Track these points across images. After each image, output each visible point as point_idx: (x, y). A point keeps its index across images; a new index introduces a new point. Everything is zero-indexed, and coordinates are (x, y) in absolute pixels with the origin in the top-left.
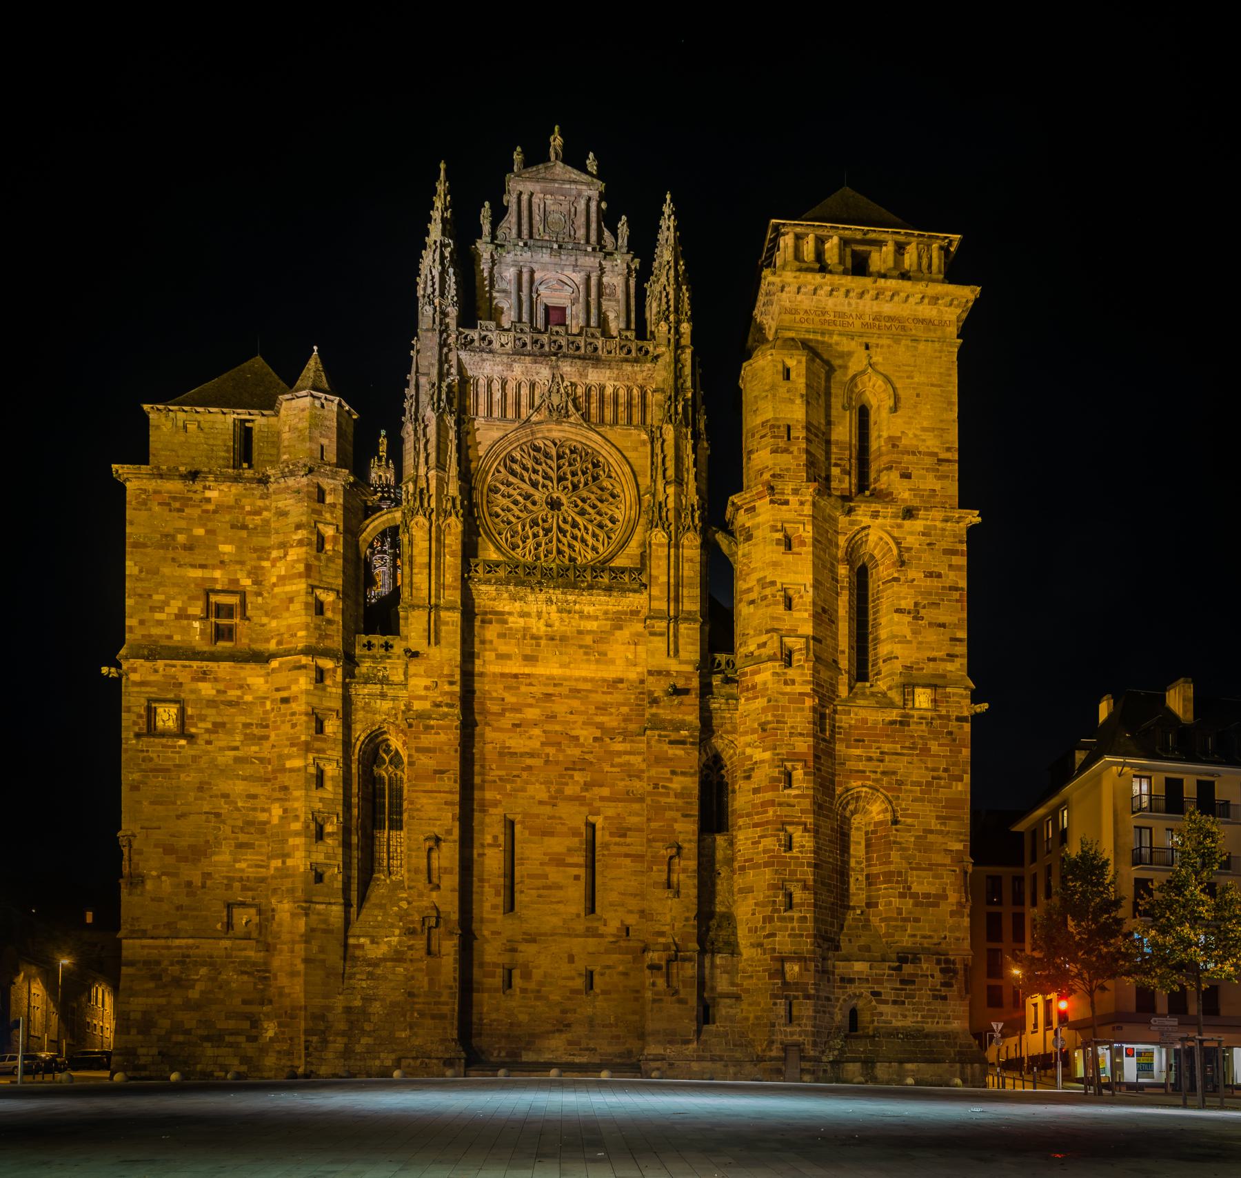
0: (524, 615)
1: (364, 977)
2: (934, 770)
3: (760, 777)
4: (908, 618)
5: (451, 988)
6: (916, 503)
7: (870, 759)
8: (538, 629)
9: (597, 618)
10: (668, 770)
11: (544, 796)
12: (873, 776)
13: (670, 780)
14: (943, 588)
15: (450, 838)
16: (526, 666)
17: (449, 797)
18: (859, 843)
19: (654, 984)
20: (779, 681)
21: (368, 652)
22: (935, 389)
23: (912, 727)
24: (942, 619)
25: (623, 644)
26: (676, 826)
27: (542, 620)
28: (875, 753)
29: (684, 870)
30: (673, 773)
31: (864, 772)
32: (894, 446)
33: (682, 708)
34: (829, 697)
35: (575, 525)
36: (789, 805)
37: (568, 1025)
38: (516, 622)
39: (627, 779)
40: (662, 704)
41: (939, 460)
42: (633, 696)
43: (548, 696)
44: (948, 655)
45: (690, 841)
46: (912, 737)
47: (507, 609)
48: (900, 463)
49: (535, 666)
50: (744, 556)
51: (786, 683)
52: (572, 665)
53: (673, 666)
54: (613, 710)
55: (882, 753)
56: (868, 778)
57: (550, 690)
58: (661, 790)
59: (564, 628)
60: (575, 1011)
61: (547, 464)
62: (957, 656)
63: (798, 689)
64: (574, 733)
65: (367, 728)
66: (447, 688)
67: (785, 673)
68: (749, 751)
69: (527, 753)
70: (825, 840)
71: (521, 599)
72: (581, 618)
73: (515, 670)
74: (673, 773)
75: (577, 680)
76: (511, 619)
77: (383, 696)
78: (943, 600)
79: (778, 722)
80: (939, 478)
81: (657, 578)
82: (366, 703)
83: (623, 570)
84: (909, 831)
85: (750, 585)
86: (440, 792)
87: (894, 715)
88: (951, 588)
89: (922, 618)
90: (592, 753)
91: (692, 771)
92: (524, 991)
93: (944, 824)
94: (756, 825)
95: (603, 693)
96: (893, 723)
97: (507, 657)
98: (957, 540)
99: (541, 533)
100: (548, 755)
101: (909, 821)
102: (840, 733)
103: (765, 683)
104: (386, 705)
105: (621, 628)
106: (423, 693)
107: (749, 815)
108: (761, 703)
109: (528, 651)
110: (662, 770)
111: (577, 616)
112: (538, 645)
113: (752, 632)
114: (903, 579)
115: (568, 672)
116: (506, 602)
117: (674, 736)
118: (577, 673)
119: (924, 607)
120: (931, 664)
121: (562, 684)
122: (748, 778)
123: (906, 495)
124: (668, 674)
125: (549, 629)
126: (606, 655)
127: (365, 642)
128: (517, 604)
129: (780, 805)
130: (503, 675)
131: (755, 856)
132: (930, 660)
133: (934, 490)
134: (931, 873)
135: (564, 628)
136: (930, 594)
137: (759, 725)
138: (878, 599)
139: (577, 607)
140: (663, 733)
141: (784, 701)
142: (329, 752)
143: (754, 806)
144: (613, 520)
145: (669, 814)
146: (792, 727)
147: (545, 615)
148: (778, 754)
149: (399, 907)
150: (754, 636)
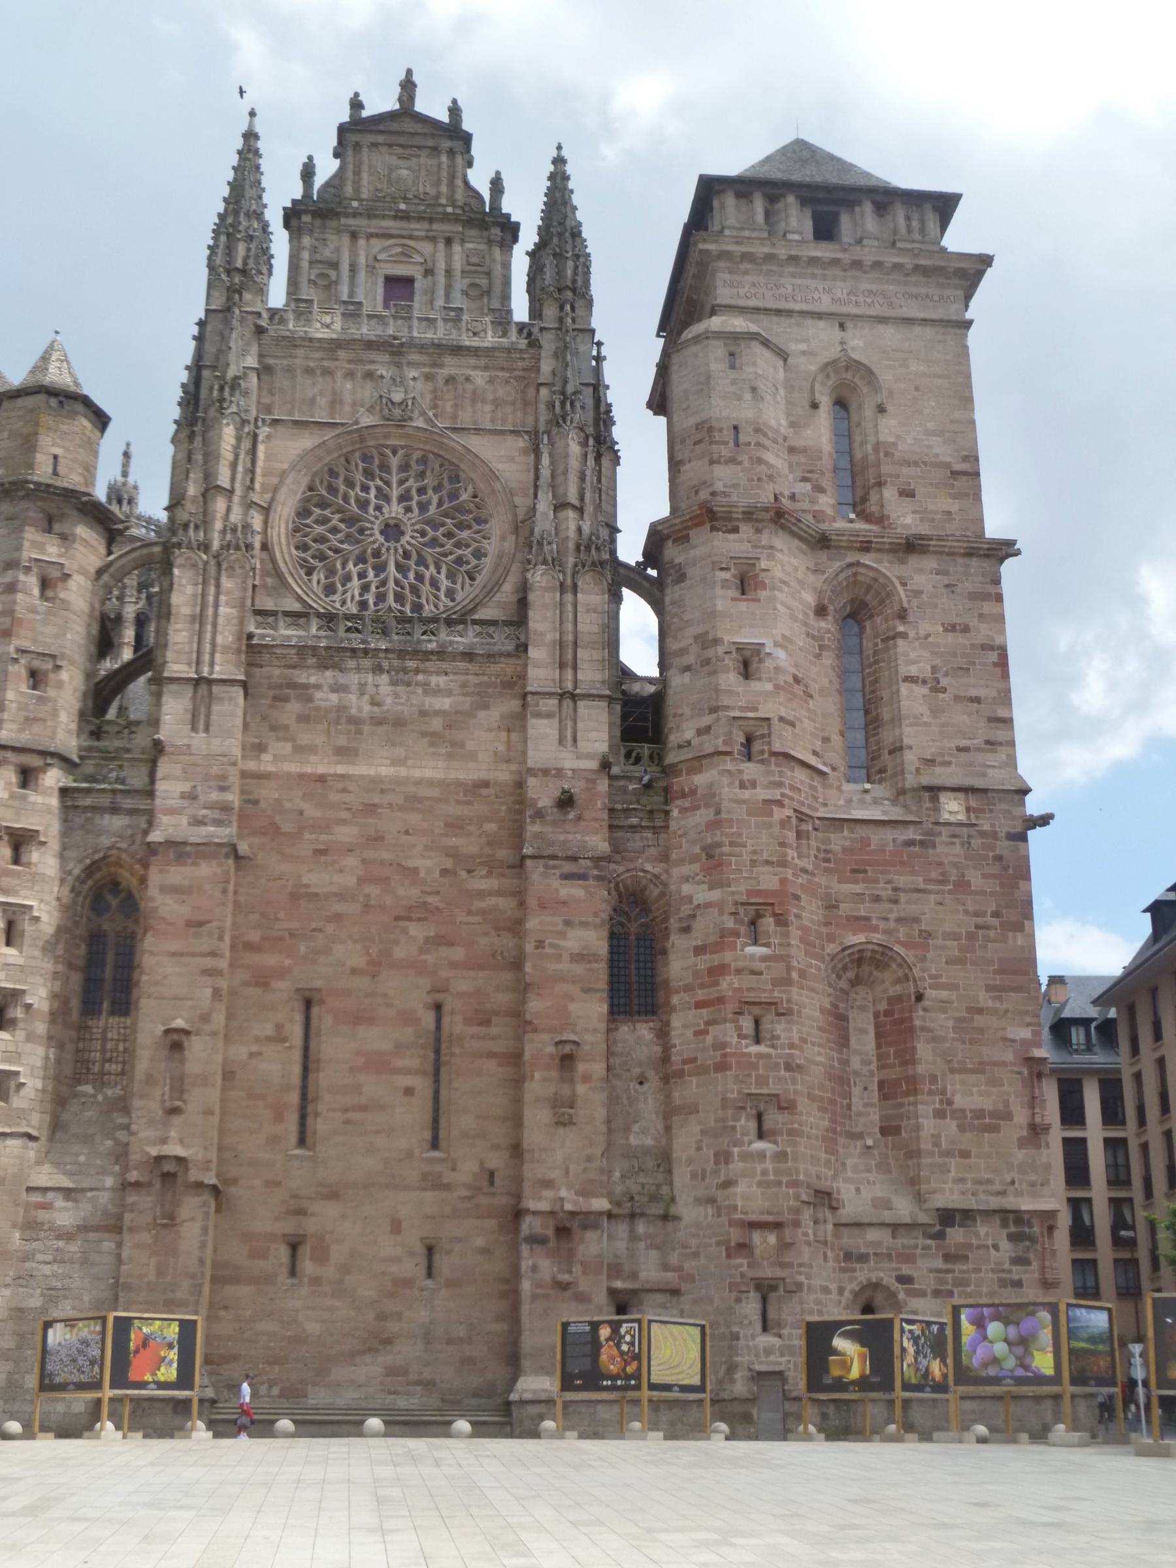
0: (338, 688)
1: (49, 1258)
2: (977, 914)
3: (704, 929)
4: (925, 690)
5: (193, 1276)
6: (924, 529)
7: (877, 899)
8: (360, 709)
9: (449, 693)
10: (559, 920)
11: (359, 961)
12: (882, 925)
13: (562, 935)
14: (973, 645)
15: (207, 1028)
16: (338, 763)
17: (209, 962)
18: (864, 1031)
19: (534, 1269)
20: (730, 784)
21: (96, 744)
22: (940, 381)
23: (938, 850)
24: (973, 693)
25: (490, 730)
26: (572, 1007)
27: (367, 697)
28: (886, 892)
29: (587, 1078)
30: (567, 923)
31: (867, 919)
32: (886, 454)
33: (582, 823)
34: (810, 807)
35: (421, 561)
36: (753, 972)
37: (388, 1341)
38: (326, 698)
39: (493, 933)
40: (549, 818)
41: (952, 473)
42: (504, 808)
43: (371, 809)
44: (987, 742)
45: (595, 1030)
46: (940, 864)
47: (313, 680)
48: (898, 476)
49: (353, 763)
50: (673, 603)
51: (742, 786)
52: (410, 762)
53: (568, 761)
54: (472, 828)
55: (895, 889)
56: (875, 929)
57: (376, 799)
58: (548, 950)
59: (400, 707)
60: (399, 1316)
61: (381, 479)
62: (1001, 744)
63: (761, 794)
64: (411, 863)
65: (86, 857)
66: (215, 796)
67: (740, 772)
68: (686, 889)
69: (336, 895)
70: (812, 1027)
71: (334, 667)
72: (426, 692)
73: (321, 770)
74: (567, 923)
75: (418, 783)
76: (318, 695)
77: (114, 810)
78: (974, 663)
79: (732, 844)
80: (955, 497)
81: (543, 634)
82: (87, 819)
83: (493, 623)
84: (945, 1011)
85: (683, 644)
86: (194, 955)
87: (911, 834)
88: (983, 647)
89: (944, 690)
90: (438, 893)
91: (598, 921)
92: (316, 1281)
93: (1000, 998)
94: (699, 1005)
95: (459, 802)
96: (910, 843)
97: (311, 749)
98: (988, 580)
99: (371, 574)
100: (368, 896)
101: (944, 994)
102: (827, 860)
103: (710, 786)
104: (118, 822)
105: (486, 707)
106: (174, 802)
107: (688, 989)
108: (703, 815)
109: (342, 741)
110: (549, 919)
111: (419, 690)
112: (359, 732)
113: (687, 712)
114: (912, 634)
115: (403, 772)
116: (313, 671)
117: (568, 867)
118: (417, 773)
119: (946, 674)
120: (963, 756)
121: (393, 790)
122: (687, 930)
123: (909, 520)
124: (560, 772)
125: (376, 709)
126: (462, 745)
127: (93, 728)
128: (329, 673)
129: (739, 971)
130: (302, 776)
131: (699, 1055)
132: (959, 749)
133: (949, 513)
134: (983, 1078)
135: (400, 707)
136: (954, 655)
137: (703, 849)
138: (876, 662)
139: (420, 677)
140: (551, 863)
141: (740, 812)
142: (23, 893)
143: (696, 974)
144: (479, 554)
145: (560, 988)
146: (754, 852)
147: (370, 689)
148: (733, 893)
149: (115, 1139)
150: (692, 717)
